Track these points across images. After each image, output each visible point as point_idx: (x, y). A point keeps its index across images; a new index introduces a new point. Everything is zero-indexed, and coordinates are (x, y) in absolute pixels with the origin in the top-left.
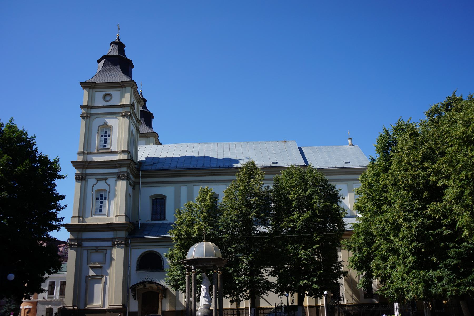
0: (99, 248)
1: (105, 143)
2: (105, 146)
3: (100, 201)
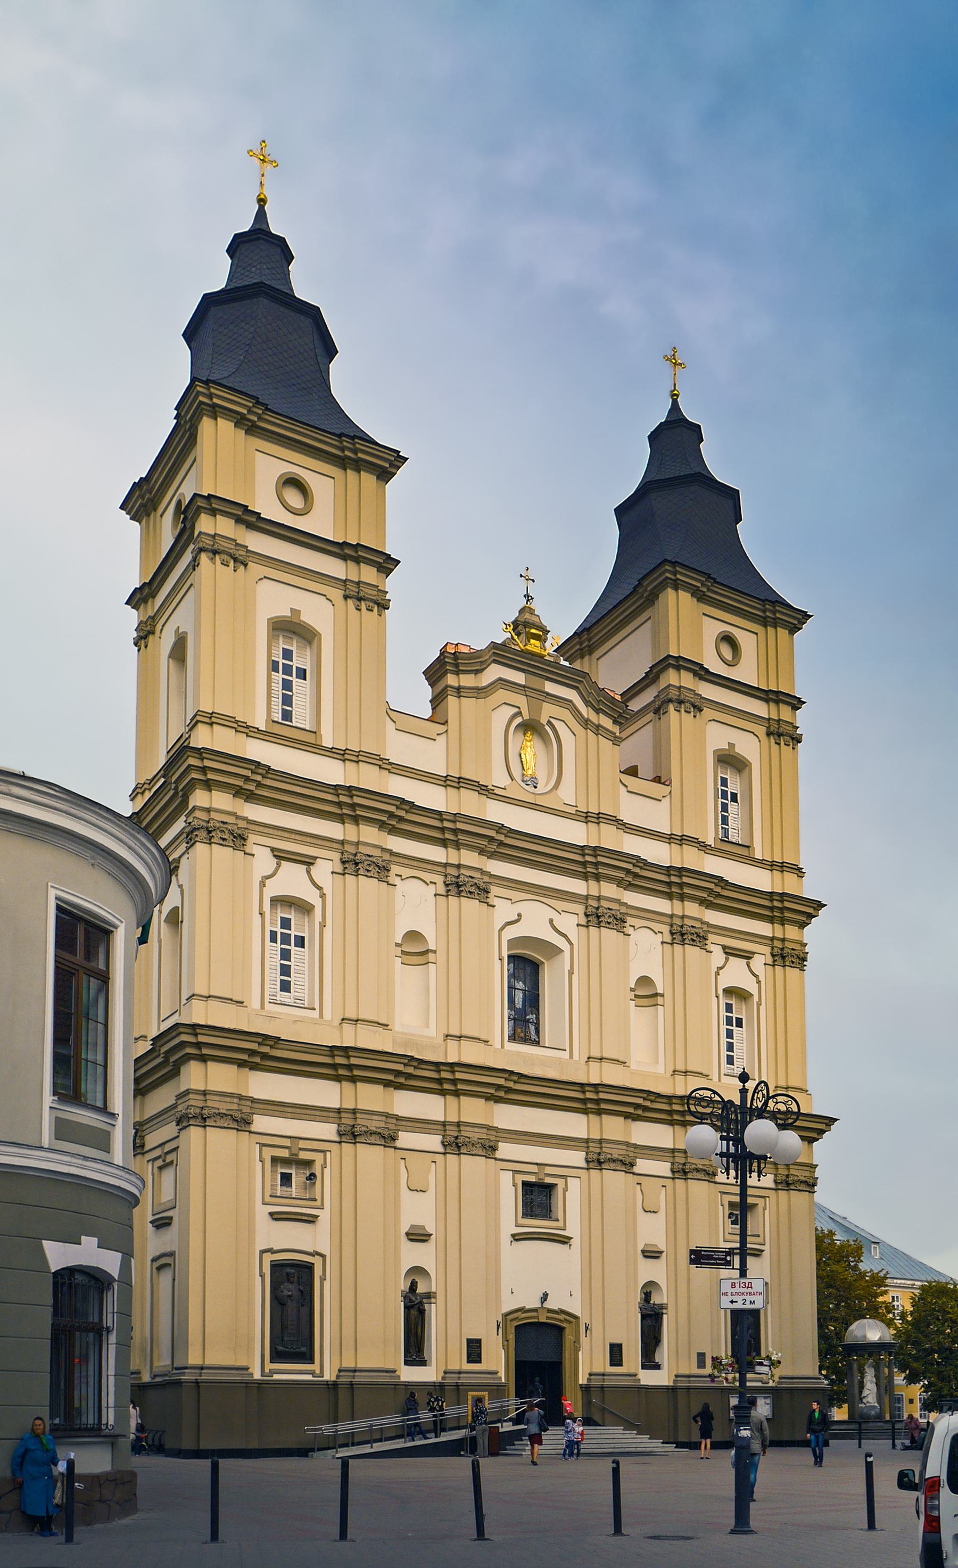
0: (302, 1144)
2: (287, 715)
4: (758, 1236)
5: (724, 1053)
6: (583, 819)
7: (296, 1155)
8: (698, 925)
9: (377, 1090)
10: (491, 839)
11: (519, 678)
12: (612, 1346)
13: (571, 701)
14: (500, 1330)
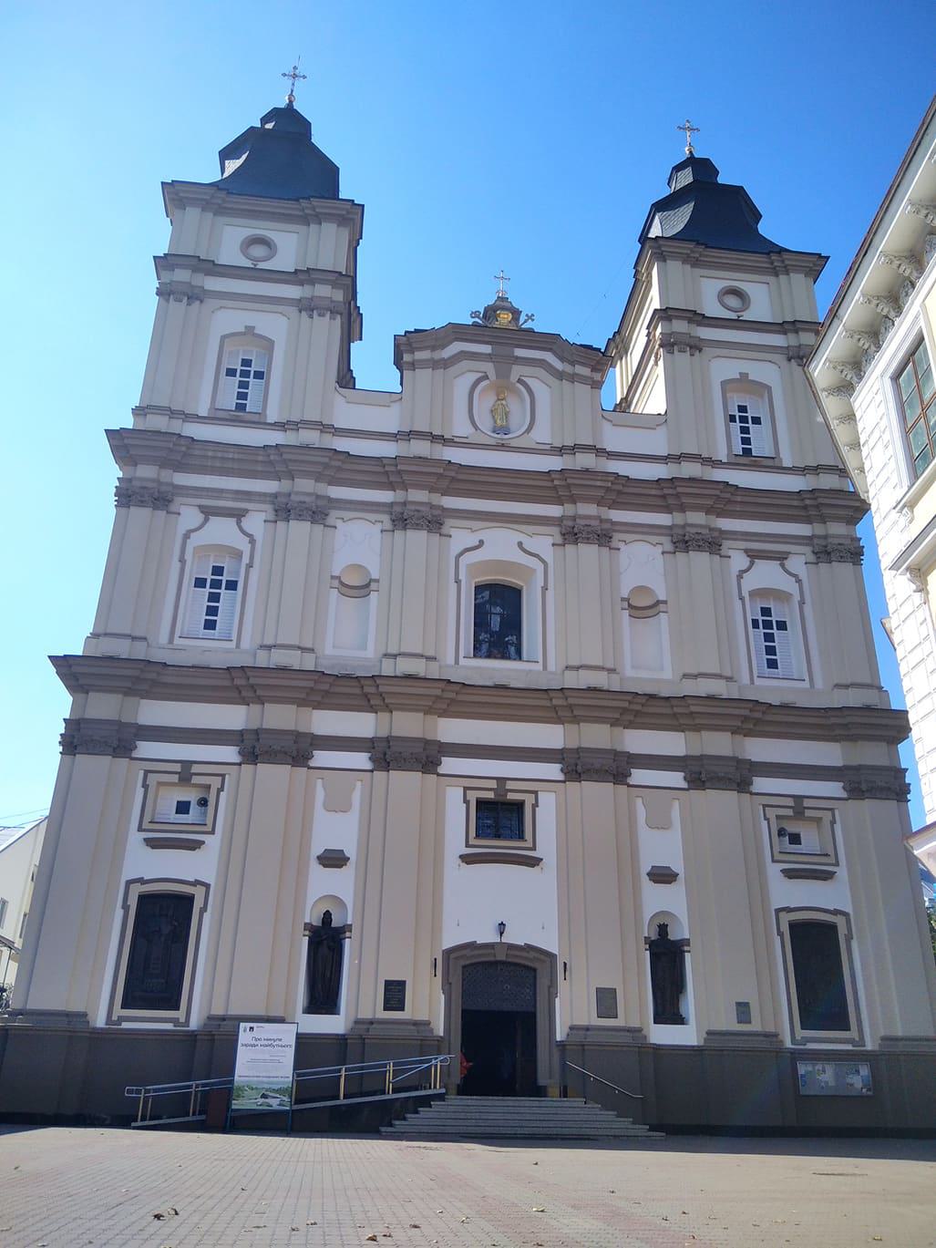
1: (242, 396)
2: (241, 407)
3: (208, 589)
4: (827, 855)
6: (558, 453)
11: (486, 349)
13: (543, 360)
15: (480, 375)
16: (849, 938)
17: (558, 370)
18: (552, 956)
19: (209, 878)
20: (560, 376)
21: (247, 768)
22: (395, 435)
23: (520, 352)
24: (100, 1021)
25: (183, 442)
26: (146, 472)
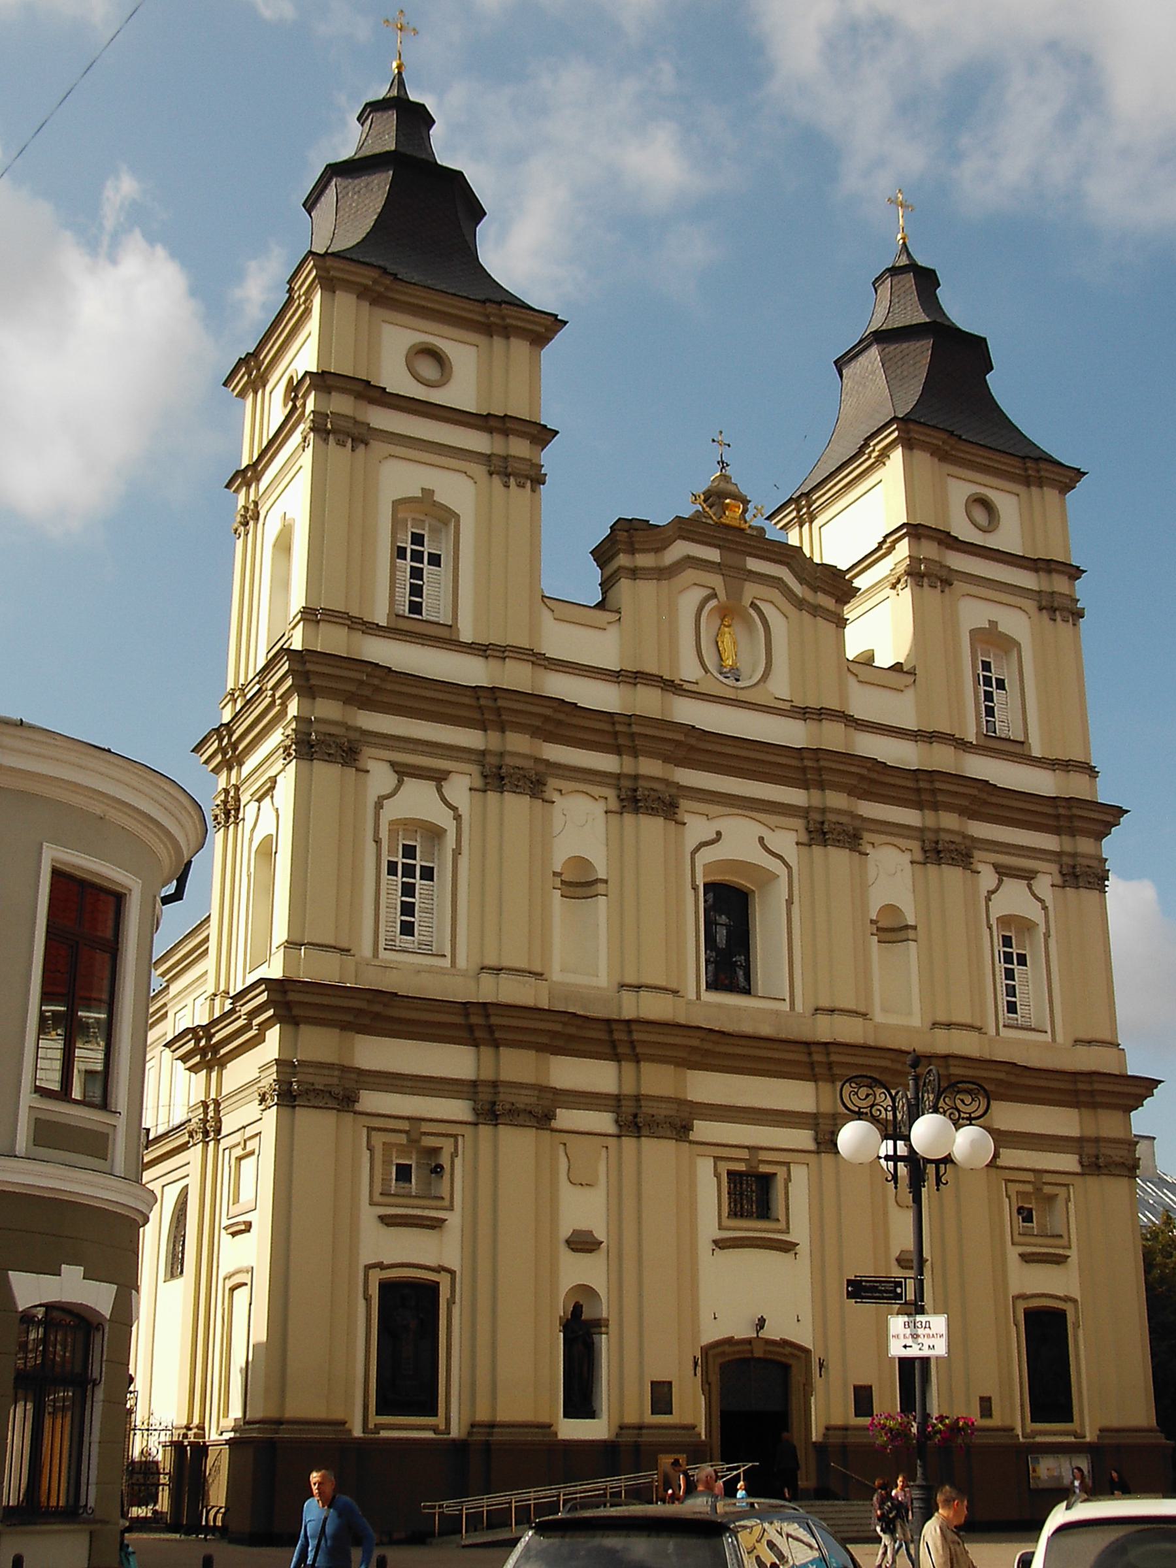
1: (416, 590)
2: (416, 608)
4: (1061, 1236)
5: (1003, 1000)
7: (418, 1141)
8: (958, 839)
9: (529, 1056)
10: (678, 743)
11: (713, 555)
12: (858, 1390)
13: (780, 579)
14: (699, 1369)
15: (709, 591)
16: (1076, 1326)
17: (796, 596)
18: (807, 1351)
19: (455, 1265)
20: (800, 604)
21: (485, 1131)
22: (618, 674)
23: (754, 564)
24: (357, 1432)
25: (378, 672)
26: (328, 709)
